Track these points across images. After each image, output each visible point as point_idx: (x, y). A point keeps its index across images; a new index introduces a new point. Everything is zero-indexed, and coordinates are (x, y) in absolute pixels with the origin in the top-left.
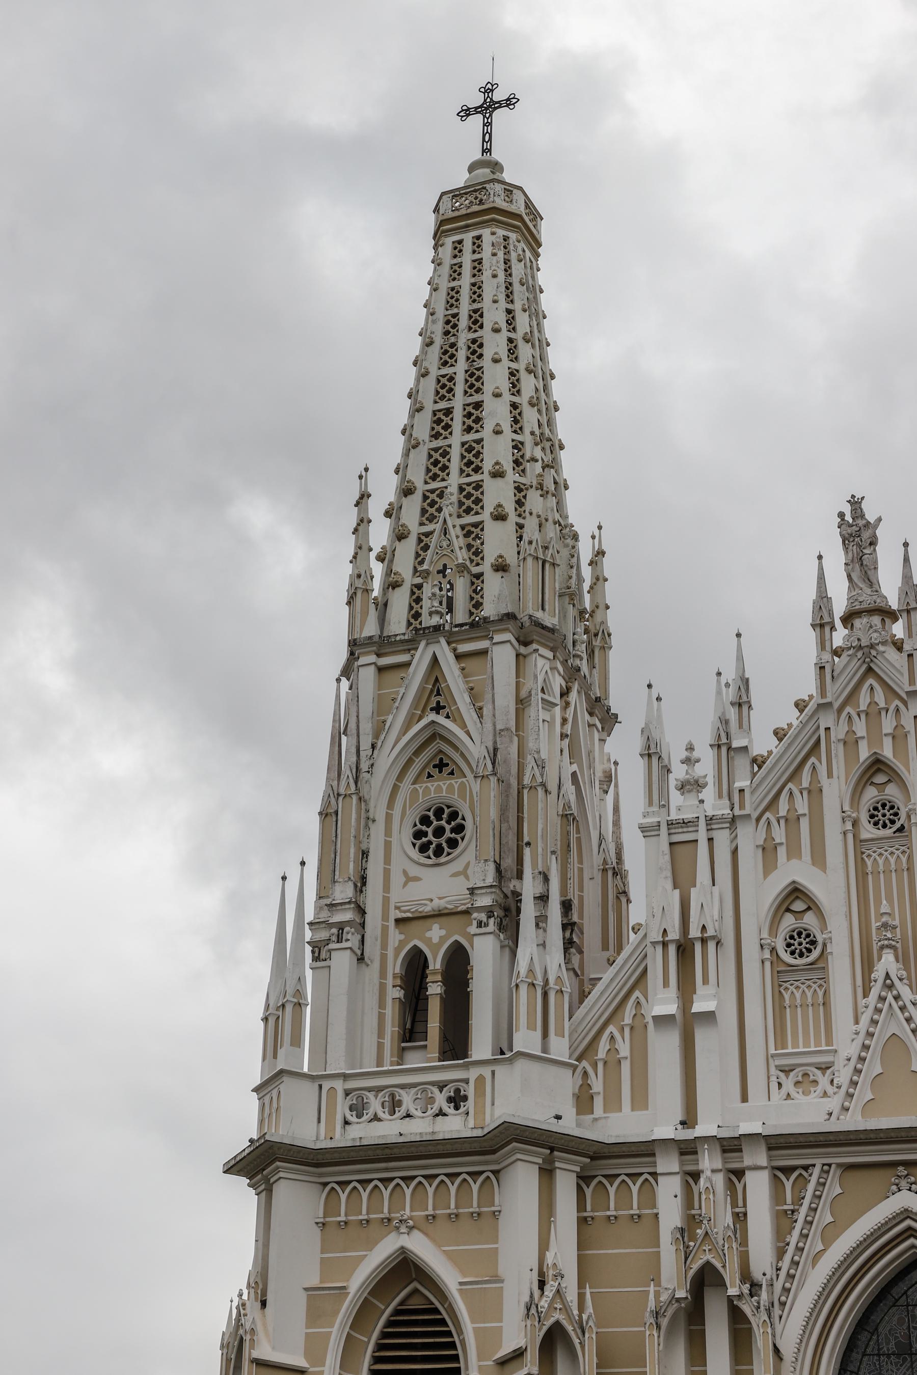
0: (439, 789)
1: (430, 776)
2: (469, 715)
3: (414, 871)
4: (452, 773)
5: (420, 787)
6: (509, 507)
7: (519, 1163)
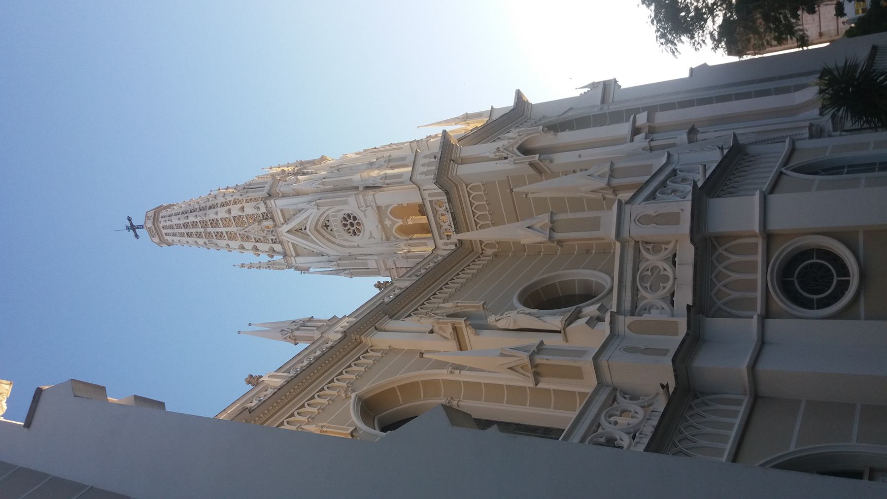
0: (336, 226)
1: (331, 230)
2: (305, 215)
3: (367, 234)
4: (328, 221)
5: (336, 234)
6: (226, 208)
7: (457, 174)
